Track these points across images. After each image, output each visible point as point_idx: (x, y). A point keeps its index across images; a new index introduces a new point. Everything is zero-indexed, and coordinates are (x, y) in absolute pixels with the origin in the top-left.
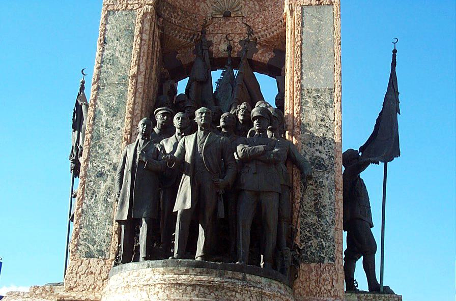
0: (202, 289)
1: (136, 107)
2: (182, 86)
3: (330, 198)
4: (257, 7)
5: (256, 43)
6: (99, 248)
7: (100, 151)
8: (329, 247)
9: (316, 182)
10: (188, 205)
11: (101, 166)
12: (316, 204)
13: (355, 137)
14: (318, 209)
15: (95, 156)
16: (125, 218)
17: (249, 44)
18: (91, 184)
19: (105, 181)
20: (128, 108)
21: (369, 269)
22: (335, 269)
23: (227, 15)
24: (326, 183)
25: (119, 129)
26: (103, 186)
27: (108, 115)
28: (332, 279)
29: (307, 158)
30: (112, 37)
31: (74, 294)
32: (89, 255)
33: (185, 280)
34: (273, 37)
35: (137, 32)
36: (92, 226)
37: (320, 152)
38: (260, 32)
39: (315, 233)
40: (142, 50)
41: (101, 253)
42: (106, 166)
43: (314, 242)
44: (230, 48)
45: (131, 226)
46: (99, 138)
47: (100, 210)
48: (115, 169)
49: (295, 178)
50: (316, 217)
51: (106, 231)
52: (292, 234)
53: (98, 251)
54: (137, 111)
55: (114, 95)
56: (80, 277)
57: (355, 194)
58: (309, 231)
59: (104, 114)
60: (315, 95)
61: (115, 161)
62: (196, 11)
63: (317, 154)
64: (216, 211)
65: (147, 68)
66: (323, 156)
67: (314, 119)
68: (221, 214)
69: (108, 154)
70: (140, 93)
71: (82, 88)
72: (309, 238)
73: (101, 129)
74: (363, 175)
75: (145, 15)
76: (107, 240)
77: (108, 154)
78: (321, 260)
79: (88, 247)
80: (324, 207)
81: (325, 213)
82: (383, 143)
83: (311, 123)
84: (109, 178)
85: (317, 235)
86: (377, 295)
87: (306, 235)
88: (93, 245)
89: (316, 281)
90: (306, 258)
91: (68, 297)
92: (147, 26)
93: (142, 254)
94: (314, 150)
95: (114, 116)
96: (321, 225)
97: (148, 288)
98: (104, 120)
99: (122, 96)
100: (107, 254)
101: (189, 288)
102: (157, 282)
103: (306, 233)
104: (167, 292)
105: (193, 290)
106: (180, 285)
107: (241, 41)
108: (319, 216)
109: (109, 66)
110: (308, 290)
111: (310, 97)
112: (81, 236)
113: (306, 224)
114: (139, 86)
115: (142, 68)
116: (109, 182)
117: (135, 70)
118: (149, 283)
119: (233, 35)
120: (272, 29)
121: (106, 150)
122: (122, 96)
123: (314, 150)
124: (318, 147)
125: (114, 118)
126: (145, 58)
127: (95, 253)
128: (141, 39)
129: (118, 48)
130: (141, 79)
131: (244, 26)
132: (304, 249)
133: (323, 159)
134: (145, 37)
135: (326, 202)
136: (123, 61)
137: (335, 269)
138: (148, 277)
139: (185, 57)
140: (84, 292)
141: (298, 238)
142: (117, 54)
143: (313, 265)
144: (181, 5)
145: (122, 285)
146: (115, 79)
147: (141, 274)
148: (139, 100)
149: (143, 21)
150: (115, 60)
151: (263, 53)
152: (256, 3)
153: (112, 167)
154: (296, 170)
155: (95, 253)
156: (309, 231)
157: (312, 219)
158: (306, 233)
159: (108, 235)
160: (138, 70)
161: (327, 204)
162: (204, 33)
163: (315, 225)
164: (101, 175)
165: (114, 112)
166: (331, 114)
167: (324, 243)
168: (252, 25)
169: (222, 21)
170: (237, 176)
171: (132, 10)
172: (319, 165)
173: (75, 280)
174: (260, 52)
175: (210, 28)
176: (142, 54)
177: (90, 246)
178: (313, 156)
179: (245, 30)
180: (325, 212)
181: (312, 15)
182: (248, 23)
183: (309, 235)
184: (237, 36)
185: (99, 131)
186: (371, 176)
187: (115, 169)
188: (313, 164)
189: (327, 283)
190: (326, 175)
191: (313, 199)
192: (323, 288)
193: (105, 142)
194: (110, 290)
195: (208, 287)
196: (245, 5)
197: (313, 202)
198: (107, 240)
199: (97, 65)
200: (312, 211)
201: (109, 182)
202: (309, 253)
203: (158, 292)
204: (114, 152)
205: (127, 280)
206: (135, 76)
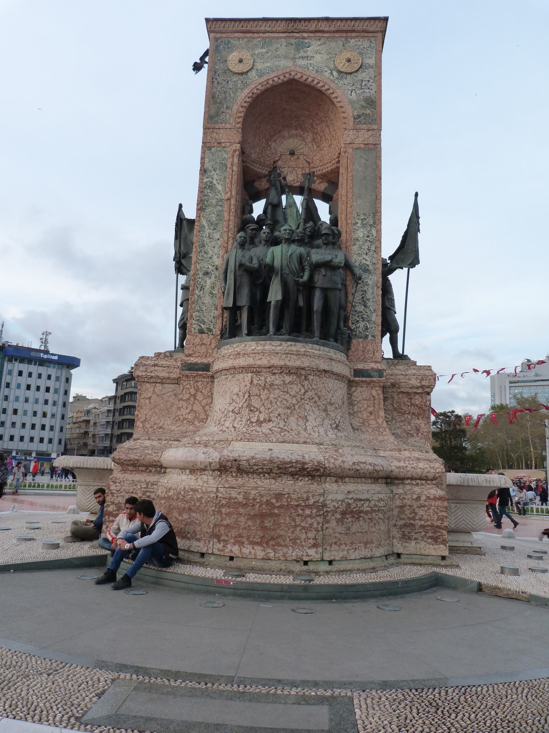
0: (292, 356)
1: (231, 223)
2: (258, 208)
3: (373, 293)
4: (315, 147)
5: (314, 176)
6: (208, 327)
7: (205, 256)
8: (372, 328)
9: (363, 282)
10: (279, 297)
11: (207, 267)
12: (363, 297)
14: (364, 301)
15: (202, 260)
16: (231, 305)
17: (310, 176)
18: (200, 280)
19: (210, 278)
21: (393, 342)
22: (376, 343)
23: (292, 153)
24: (370, 282)
25: (219, 239)
27: (210, 229)
28: (374, 350)
29: (357, 264)
30: (210, 168)
31: (192, 359)
32: (201, 332)
33: (281, 350)
34: (328, 172)
35: (229, 166)
36: (202, 311)
37: (366, 260)
38: (317, 167)
39: (362, 318)
40: (233, 179)
41: (210, 330)
42: (210, 267)
43: (362, 324)
45: (234, 311)
46: (203, 246)
47: (207, 300)
48: (217, 269)
49: (348, 279)
50: (363, 307)
51: (212, 314)
52: (346, 319)
53: (208, 329)
54: (231, 226)
55: (213, 213)
56: (196, 346)
57: (386, 290)
58: (358, 317)
59: (207, 227)
60: (362, 217)
61: (216, 264)
62: (269, 149)
63: (364, 261)
64: (297, 301)
65: (237, 194)
66: (368, 263)
67: (361, 235)
68: (301, 303)
69: (211, 258)
70: (233, 212)
72: (358, 321)
73: (205, 239)
74: (390, 277)
75: (235, 151)
76: (214, 321)
77: (211, 258)
78: (367, 337)
79: (200, 326)
80: (368, 299)
81: (370, 304)
82: (408, 253)
83: (359, 239)
84: (213, 276)
85: (363, 321)
86: (400, 361)
87: (356, 319)
88: (204, 325)
89: (363, 351)
90: (356, 335)
91: (188, 360)
92: (236, 160)
93: (245, 331)
94: (362, 258)
95: (214, 229)
96: (367, 312)
97: (254, 355)
98: (207, 232)
100: (214, 330)
101: (284, 356)
102: (260, 351)
103: (356, 318)
104: (268, 358)
105: (286, 357)
106: (277, 353)
107: (302, 173)
108: (365, 306)
109: (209, 191)
110: (357, 357)
111: (359, 219)
112: (195, 318)
113: (356, 311)
114: (232, 207)
115: (234, 193)
116: (213, 278)
117: (229, 195)
118: (254, 352)
119: (297, 169)
120: (328, 165)
121: (210, 255)
122: (219, 215)
123: (362, 258)
124: (365, 256)
125: (215, 231)
126: (236, 185)
127: (205, 330)
128: (232, 171)
129: (216, 177)
130: (233, 201)
131: (305, 162)
132: (354, 329)
133: (368, 265)
134: (235, 168)
135: (369, 295)
136: (220, 187)
137: (376, 343)
138: (253, 348)
139: (263, 184)
140: (199, 358)
141: (350, 321)
142: (215, 182)
143: (362, 339)
144: (258, 144)
145: (234, 353)
146: (214, 201)
147: (247, 346)
148: (232, 218)
149: (233, 156)
150: (213, 186)
151: (320, 183)
152: (314, 144)
153: (214, 268)
154: (349, 273)
155: (205, 330)
156: (358, 317)
158: (356, 318)
159: (214, 317)
160: (231, 194)
161: (371, 297)
162: (275, 168)
163: (362, 312)
164: (207, 273)
165: (214, 226)
166: (374, 232)
167: (368, 325)
168: (311, 161)
169: (289, 157)
170: (311, 277)
171: (224, 147)
172: (366, 271)
173: (192, 349)
174: (317, 182)
175: (280, 163)
176: (233, 183)
177: (202, 325)
178: (361, 262)
179: (306, 165)
180: (369, 304)
181: (361, 156)
182: (308, 160)
183: (358, 319)
184: (300, 170)
185: (204, 241)
186: (397, 279)
187: (217, 269)
188: (360, 269)
189: (370, 352)
190: (370, 277)
191: (362, 293)
192: (367, 356)
193: (208, 248)
194: (223, 356)
195: (296, 355)
196: (306, 145)
197: (361, 296)
198: (214, 321)
200: (360, 303)
201: (213, 278)
202: (358, 332)
203: (261, 358)
204: (215, 257)
205: (236, 349)
206: (229, 199)
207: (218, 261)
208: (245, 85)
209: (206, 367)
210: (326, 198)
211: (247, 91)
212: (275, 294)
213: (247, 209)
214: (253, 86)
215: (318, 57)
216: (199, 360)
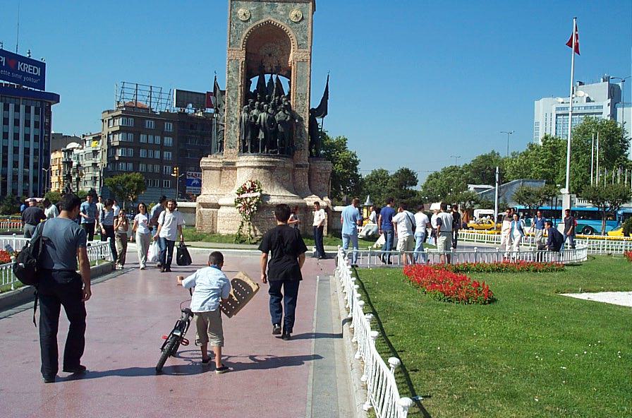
13: (315, 104)
20: (239, 98)
26: (233, 125)
32: (231, 148)
44: (271, 70)
47: (233, 133)
68: (272, 139)
71: (215, 79)
99: (237, 93)
117: (240, 84)
146: (234, 87)
157: (299, 137)
164: (232, 121)
165: (235, 99)
199: (227, 82)
206: (241, 86)
207: (237, 116)
208: (247, 27)
209: (234, 163)
210: (289, 76)
211: (247, 30)
212: (261, 135)
213: (247, 84)
214: (250, 28)
215: (282, 13)
216: (230, 161)
